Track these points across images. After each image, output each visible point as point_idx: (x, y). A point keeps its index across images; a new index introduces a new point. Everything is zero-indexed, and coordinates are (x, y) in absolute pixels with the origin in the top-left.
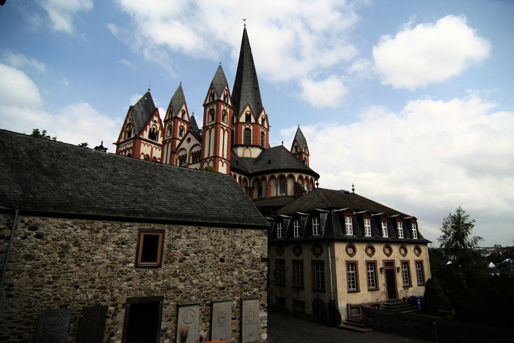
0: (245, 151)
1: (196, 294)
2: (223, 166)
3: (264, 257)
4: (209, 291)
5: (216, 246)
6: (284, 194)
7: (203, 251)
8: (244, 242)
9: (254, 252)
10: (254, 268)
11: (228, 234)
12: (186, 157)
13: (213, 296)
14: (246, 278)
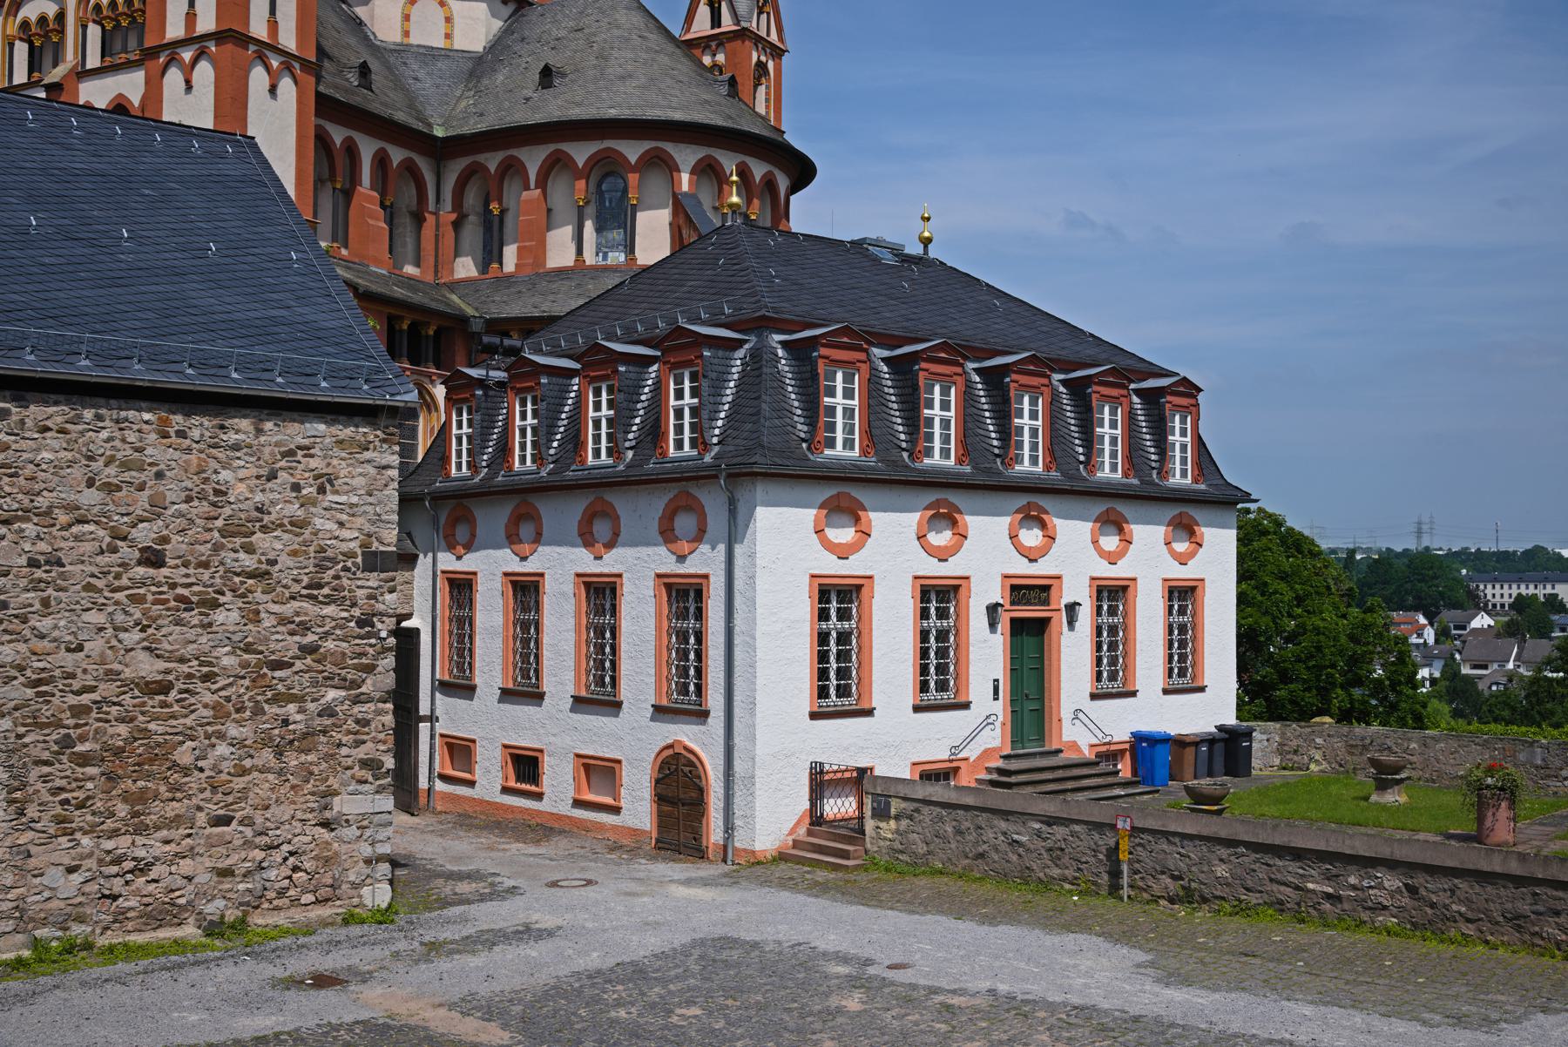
1: (16, 709)
2: (273, 90)
3: (375, 546)
4: (86, 699)
5: (119, 489)
6: (617, 257)
8: (272, 476)
10: (326, 596)
11: (181, 434)
12: (61, 31)
13: (107, 721)
14: (286, 645)
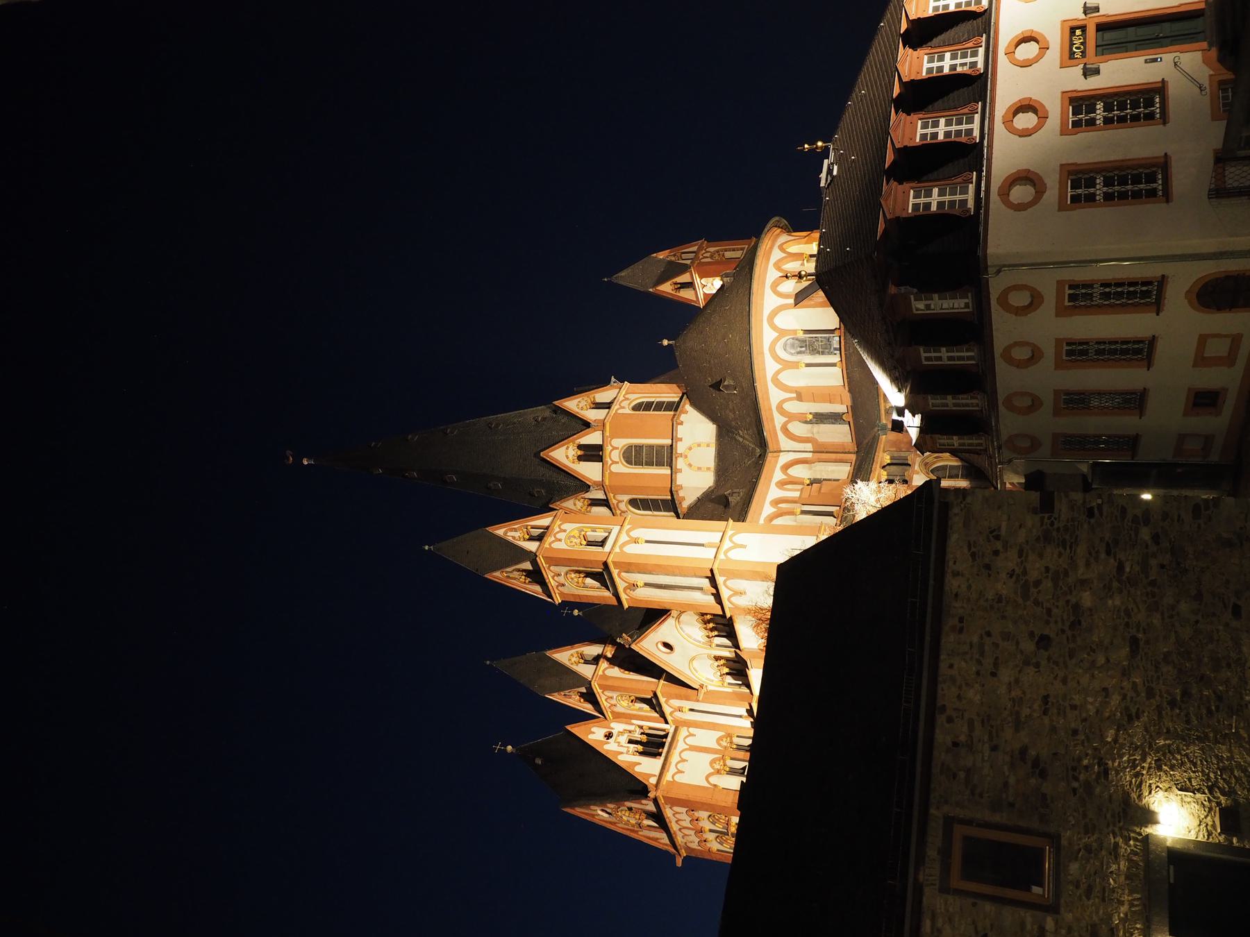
0: (695, 464)
7: (1014, 700)
9: (1022, 536)
11: (961, 620)
